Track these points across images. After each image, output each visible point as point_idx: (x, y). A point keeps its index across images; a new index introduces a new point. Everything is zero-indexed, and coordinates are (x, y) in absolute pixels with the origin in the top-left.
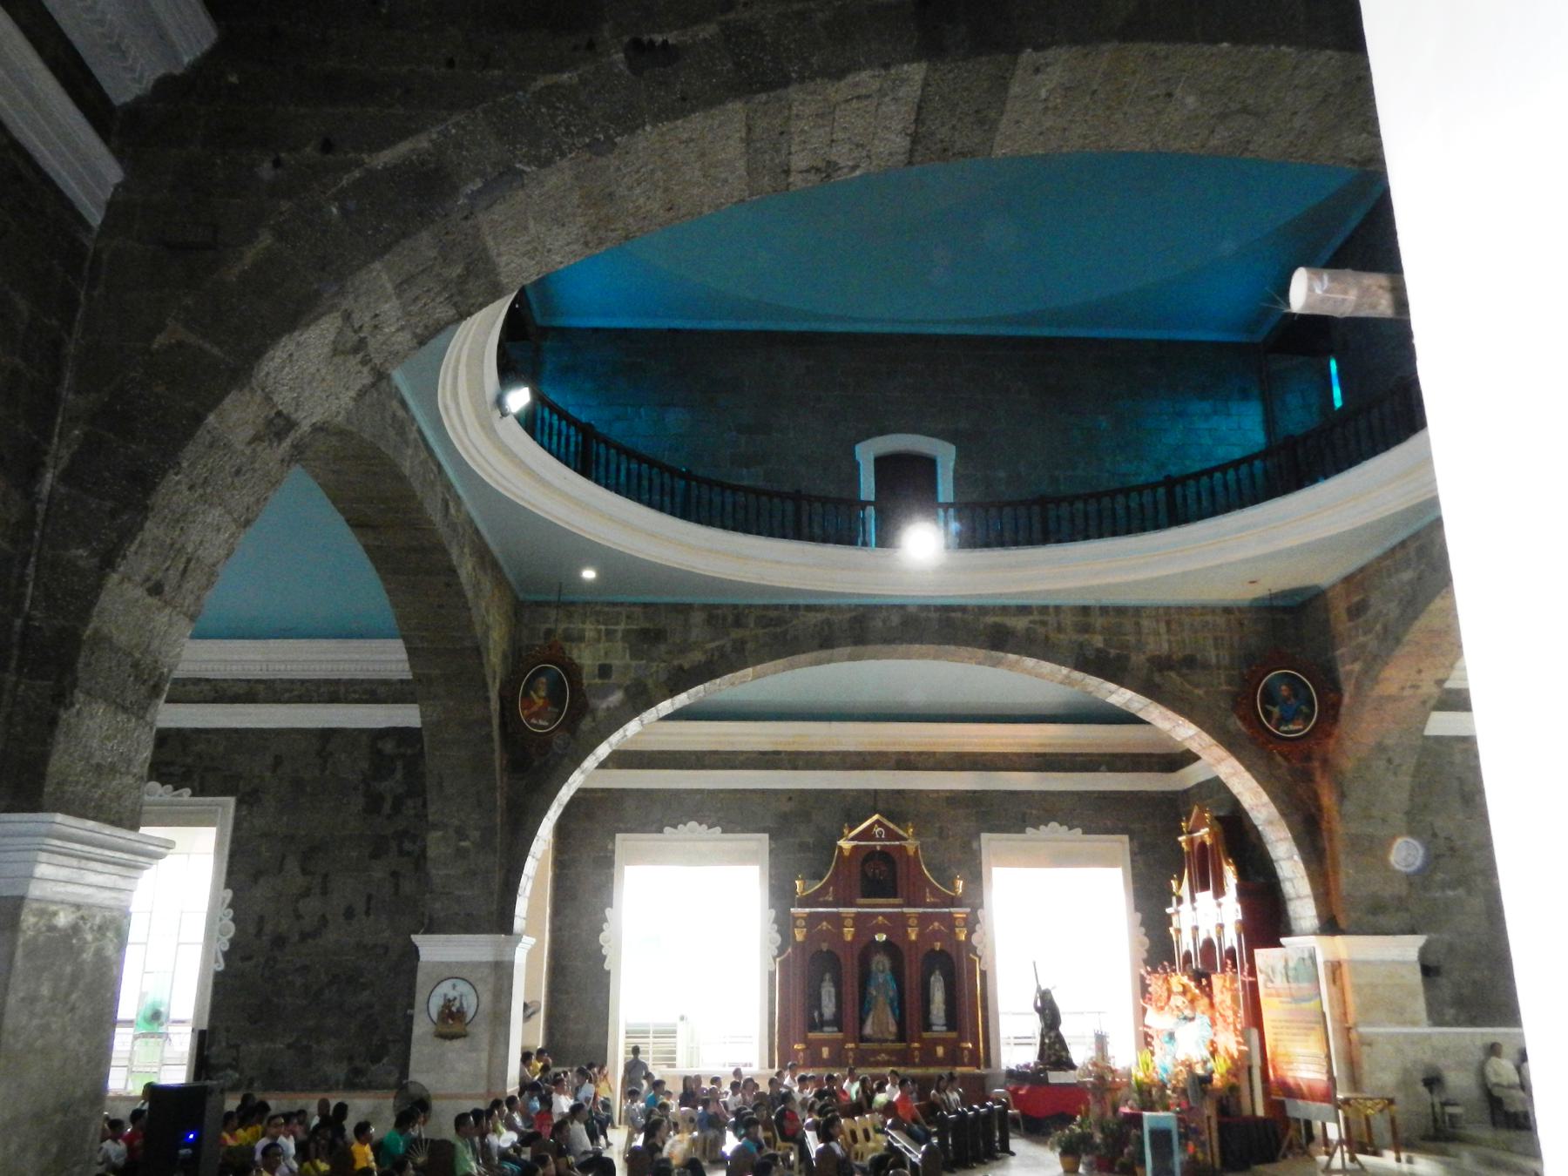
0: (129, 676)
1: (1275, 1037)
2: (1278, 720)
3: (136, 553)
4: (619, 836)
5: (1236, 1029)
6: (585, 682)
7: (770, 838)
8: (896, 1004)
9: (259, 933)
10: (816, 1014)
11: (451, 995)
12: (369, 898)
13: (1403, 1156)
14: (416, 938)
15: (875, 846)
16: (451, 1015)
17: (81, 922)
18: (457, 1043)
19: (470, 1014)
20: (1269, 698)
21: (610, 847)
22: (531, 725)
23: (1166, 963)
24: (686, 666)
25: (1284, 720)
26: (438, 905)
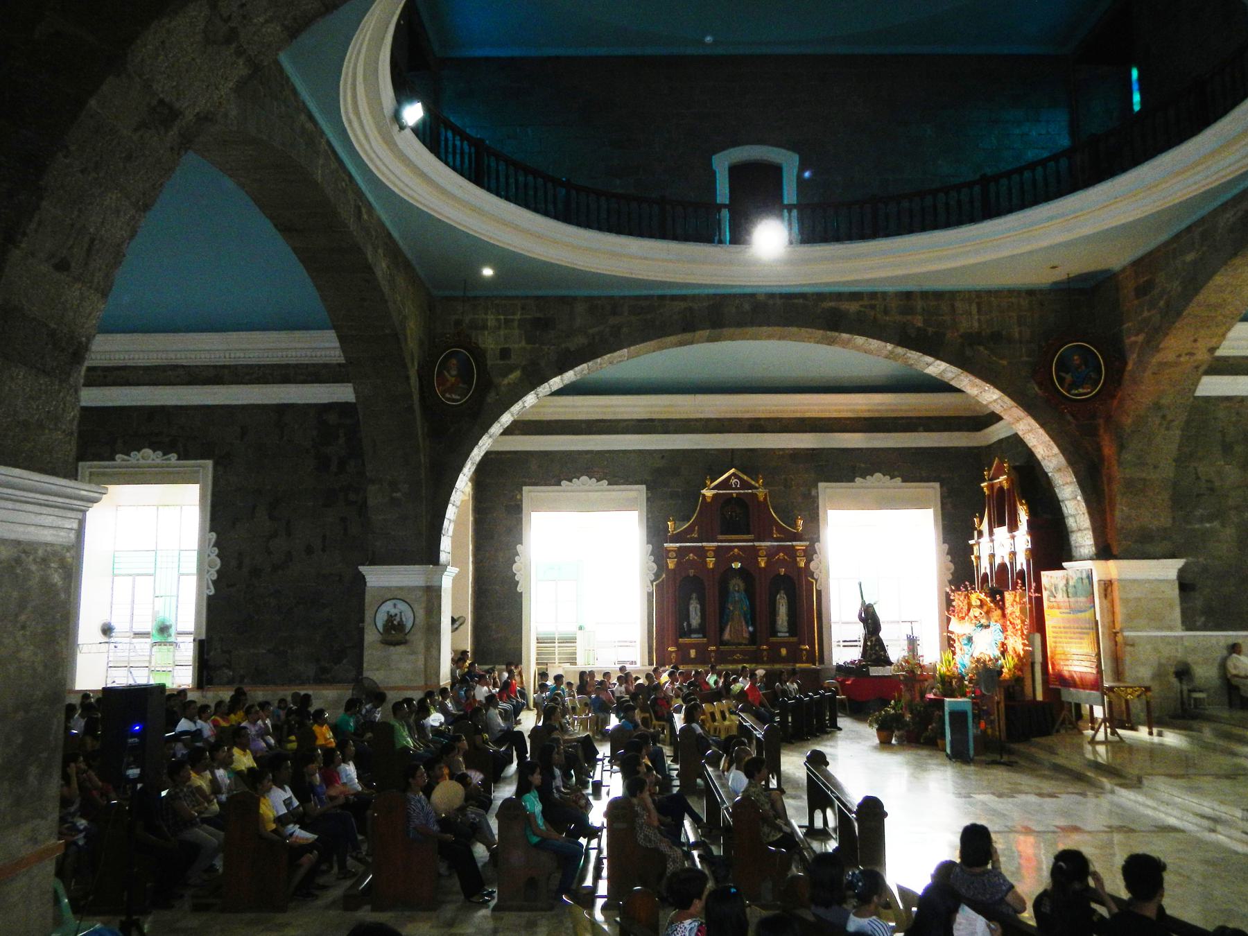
0: (47, 344)
1: (1054, 640)
2: (1069, 385)
3: (36, 231)
4: (525, 489)
5: (1023, 634)
6: (489, 363)
7: (647, 490)
8: (749, 617)
9: (240, 566)
10: (685, 624)
11: (393, 611)
12: (324, 537)
13: (1155, 730)
14: (361, 568)
15: (732, 493)
16: (393, 627)
17: (23, 555)
18: (400, 649)
19: (409, 625)
20: (1063, 365)
21: (518, 497)
22: (449, 399)
23: (967, 583)
24: (572, 349)
25: (1074, 385)
26: (378, 544)
